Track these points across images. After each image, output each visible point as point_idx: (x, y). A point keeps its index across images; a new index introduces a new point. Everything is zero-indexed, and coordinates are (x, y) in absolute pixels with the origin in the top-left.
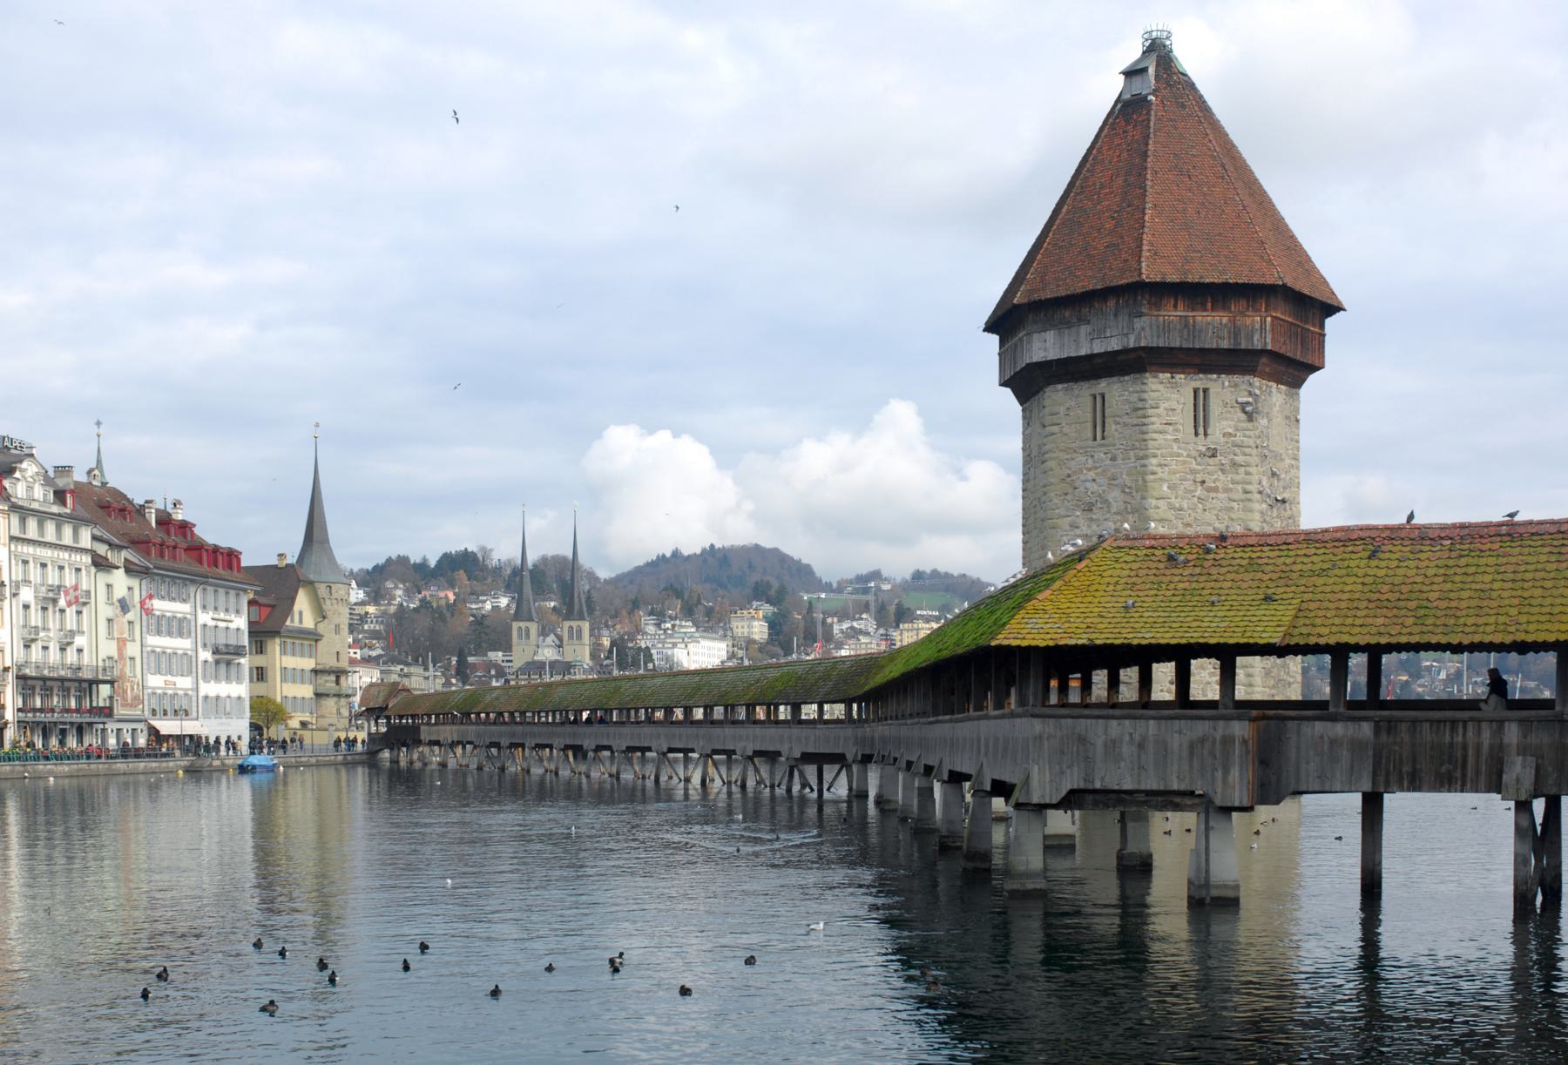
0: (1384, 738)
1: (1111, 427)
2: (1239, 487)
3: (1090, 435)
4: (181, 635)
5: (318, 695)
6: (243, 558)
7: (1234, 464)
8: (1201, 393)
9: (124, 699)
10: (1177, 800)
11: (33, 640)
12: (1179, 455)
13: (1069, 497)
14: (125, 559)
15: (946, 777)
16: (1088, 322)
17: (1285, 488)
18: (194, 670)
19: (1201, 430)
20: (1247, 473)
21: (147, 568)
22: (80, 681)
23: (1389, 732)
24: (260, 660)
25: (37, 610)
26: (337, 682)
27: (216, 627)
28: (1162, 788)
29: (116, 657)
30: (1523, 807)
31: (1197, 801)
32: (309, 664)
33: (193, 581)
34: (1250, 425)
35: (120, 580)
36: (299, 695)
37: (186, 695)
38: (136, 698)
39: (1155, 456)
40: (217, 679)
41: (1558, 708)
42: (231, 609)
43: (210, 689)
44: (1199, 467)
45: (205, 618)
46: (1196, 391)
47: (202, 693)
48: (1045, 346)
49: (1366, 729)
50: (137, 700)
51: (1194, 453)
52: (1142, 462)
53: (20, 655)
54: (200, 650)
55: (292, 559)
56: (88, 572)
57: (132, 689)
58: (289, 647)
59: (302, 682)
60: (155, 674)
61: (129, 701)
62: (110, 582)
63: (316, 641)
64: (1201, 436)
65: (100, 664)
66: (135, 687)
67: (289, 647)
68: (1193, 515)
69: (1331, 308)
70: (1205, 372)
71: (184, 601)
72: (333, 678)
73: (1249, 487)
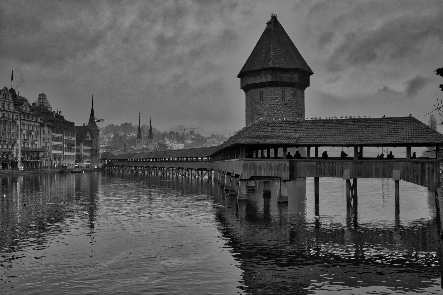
0: (318, 165)
1: (264, 98)
2: (292, 111)
3: (259, 100)
4: (60, 141)
5: (92, 155)
6: (75, 124)
7: (291, 107)
8: (283, 91)
9: (46, 156)
10: (274, 179)
11: (26, 142)
12: (279, 104)
13: (255, 113)
14: (48, 124)
15: (227, 174)
16: (259, 76)
17: (301, 112)
19: (283, 99)
20: (294, 108)
22: (36, 152)
23: (319, 164)
24: (78, 147)
25: (26, 136)
26: (96, 152)
27: (68, 140)
28: (271, 176)
30: (348, 181)
31: (279, 179)
32: (89, 148)
33: (63, 129)
34: (294, 98)
35: (46, 129)
36: (87, 155)
37: (61, 155)
38: (49, 155)
39: (274, 104)
40: (68, 151)
41: (355, 159)
43: (66, 154)
44: (283, 107)
45: (66, 138)
46: (282, 91)
47: (65, 155)
48: (250, 81)
49: (315, 163)
51: (282, 104)
52: (271, 106)
53: (22, 146)
54: (64, 145)
55: (86, 125)
57: (48, 153)
58: (85, 144)
59: (88, 152)
62: (44, 129)
63: (92, 143)
64: (283, 100)
65: (41, 148)
68: (282, 117)
69: (312, 73)
70: (284, 87)
71: (61, 134)
72: (95, 151)
73: (294, 111)
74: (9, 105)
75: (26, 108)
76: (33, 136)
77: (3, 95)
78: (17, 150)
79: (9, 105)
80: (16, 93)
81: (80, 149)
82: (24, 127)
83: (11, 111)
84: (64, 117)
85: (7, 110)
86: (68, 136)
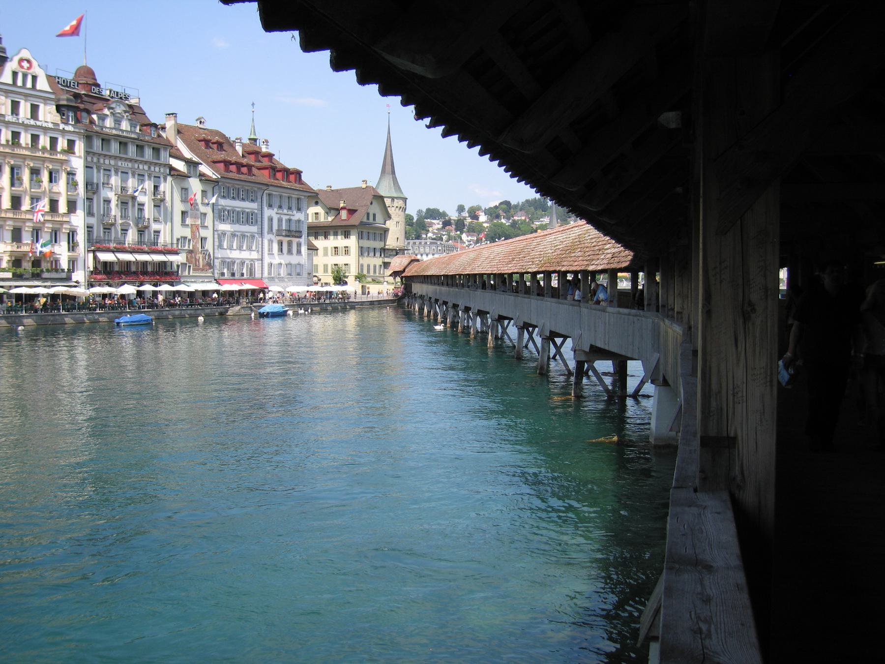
29: (189, 237)
42: (293, 208)
58: (365, 235)
62: (186, 186)
67: (365, 235)
71: (252, 200)
74: (34, 109)
75: (118, 121)
77: (15, 74)
79: (34, 109)
81: (350, 247)
83: (45, 125)
84: (274, 155)
85: (27, 122)
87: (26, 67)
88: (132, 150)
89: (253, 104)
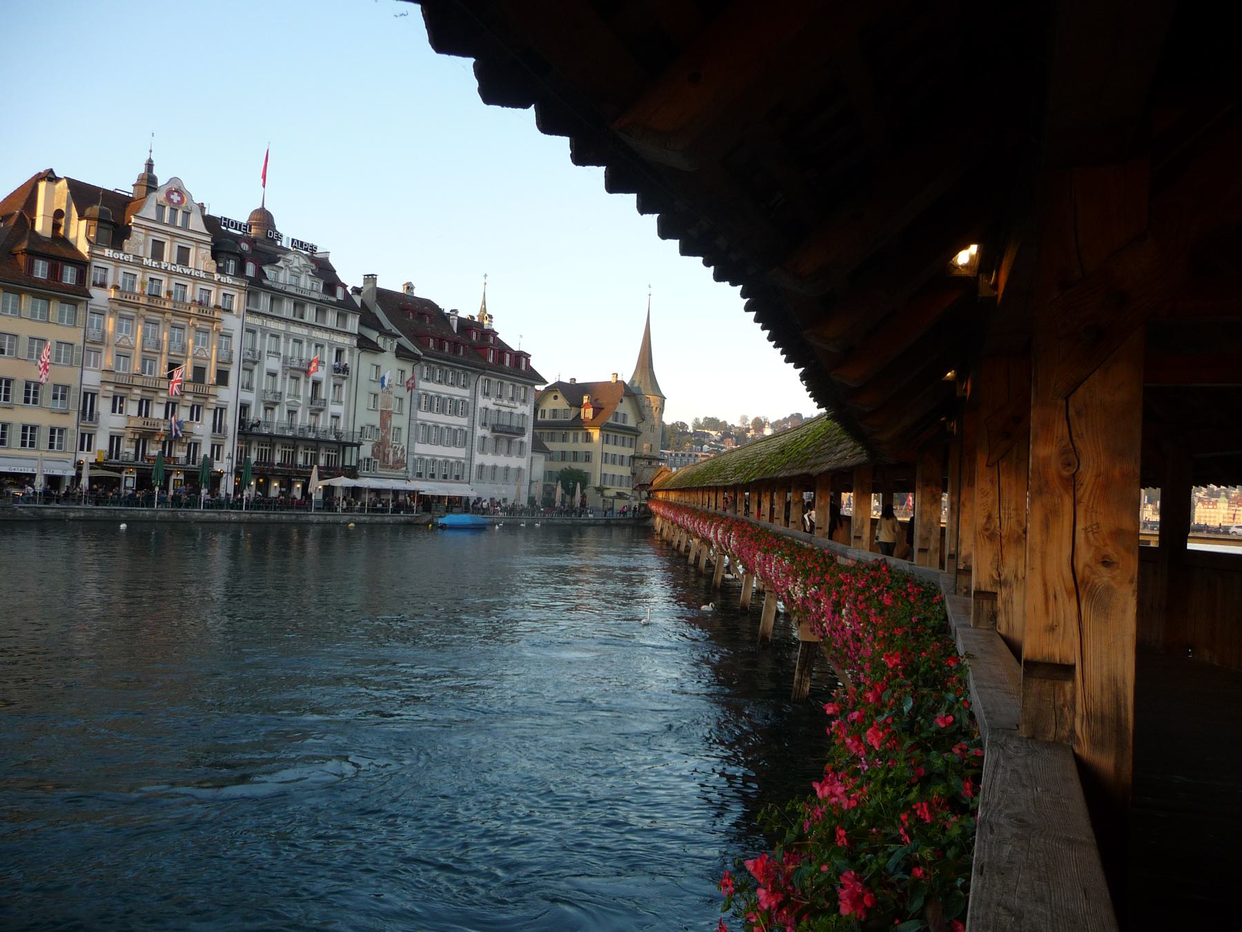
11: (276, 404)
18: (469, 443)
21: (419, 356)
25: (284, 379)
27: (499, 411)
32: (628, 452)
33: (473, 372)
40: (496, 452)
43: (489, 460)
50: (399, 464)
56: (351, 353)
57: (395, 453)
58: (611, 439)
60: (437, 445)
61: (391, 463)
63: (637, 436)
65: (357, 429)
66: (399, 452)
67: (611, 439)
71: (464, 387)
76: (316, 384)
77: (160, 208)
78: (218, 427)
80: (274, 227)
82: (278, 345)
86: (500, 397)
87: (175, 201)
88: (310, 314)
89: (486, 276)
